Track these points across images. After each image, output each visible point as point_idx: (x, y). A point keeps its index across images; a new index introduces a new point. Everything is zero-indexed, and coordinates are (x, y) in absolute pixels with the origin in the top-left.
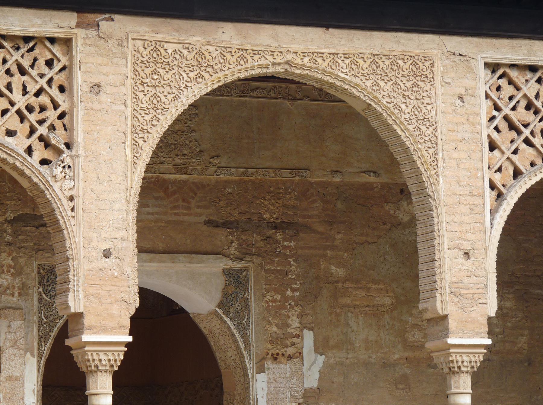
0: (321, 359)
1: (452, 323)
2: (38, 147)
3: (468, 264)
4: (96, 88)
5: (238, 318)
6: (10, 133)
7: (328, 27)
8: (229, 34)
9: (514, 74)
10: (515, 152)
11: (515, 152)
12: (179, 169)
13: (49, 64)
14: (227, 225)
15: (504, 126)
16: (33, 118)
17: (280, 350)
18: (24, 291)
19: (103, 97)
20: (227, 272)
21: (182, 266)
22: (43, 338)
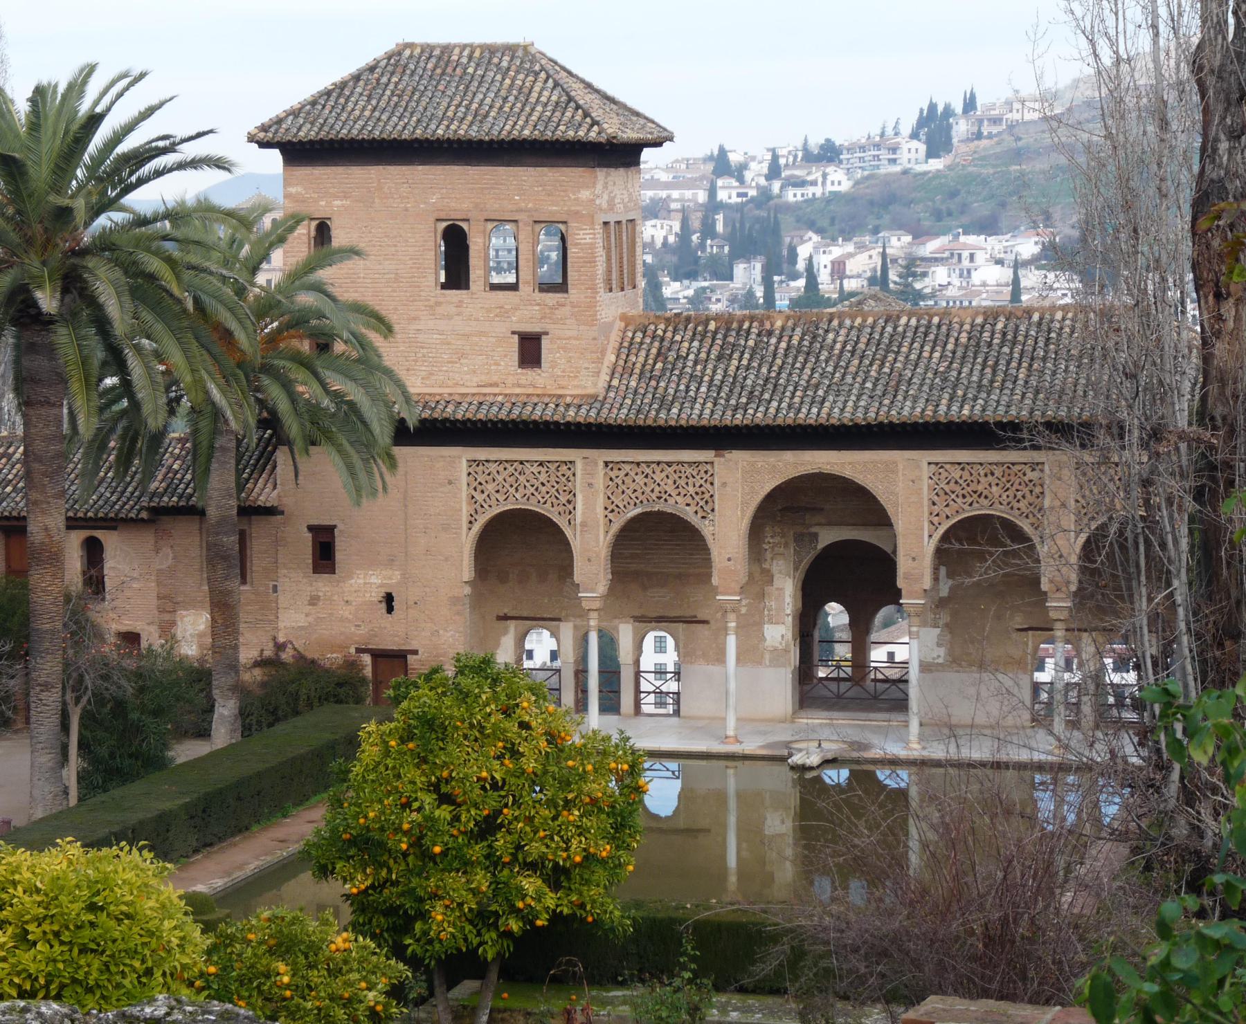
0: (950, 582)
1: (903, 592)
2: (700, 510)
3: (914, 564)
6: (688, 505)
7: (840, 449)
10: (947, 506)
11: (947, 506)
13: (706, 472)
15: (941, 493)
16: (697, 498)
18: (786, 545)
19: (728, 489)
22: (796, 569)
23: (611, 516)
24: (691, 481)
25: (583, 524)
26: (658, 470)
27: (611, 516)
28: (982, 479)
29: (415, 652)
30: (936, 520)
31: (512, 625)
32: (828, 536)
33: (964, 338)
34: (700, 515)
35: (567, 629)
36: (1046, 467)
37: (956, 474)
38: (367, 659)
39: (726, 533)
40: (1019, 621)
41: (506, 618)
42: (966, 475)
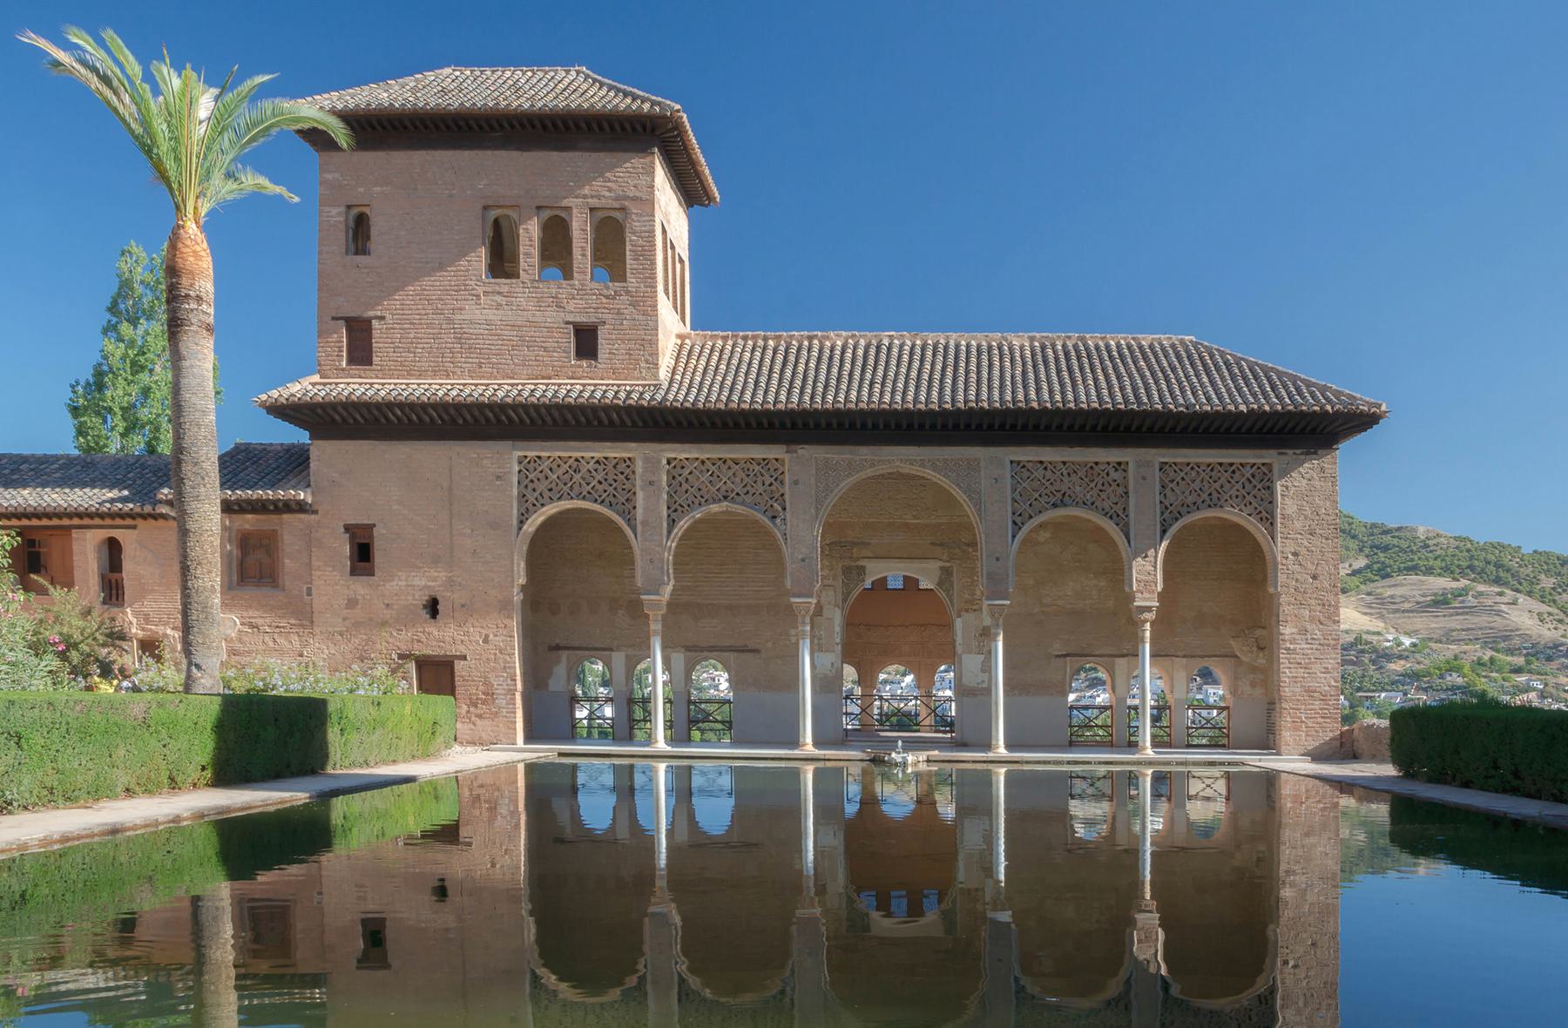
4: (796, 483)
5: (947, 591)
8: (865, 452)
9: (1029, 466)
12: (915, 517)
14: (941, 545)
17: (972, 606)
18: (835, 577)
20: (942, 568)
21: (917, 565)
22: (844, 600)
23: (674, 516)
24: (760, 479)
25: (644, 523)
26: (724, 468)
27: (674, 516)
28: (1066, 479)
29: (464, 658)
30: (1018, 520)
31: (564, 655)
32: (875, 570)
33: (1028, 353)
34: (770, 514)
35: (618, 658)
36: (1131, 468)
37: (1039, 473)
38: (412, 667)
39: (802, 534)
40: (1057, 648)
41: (558, 648)
42: (1049, 473)
